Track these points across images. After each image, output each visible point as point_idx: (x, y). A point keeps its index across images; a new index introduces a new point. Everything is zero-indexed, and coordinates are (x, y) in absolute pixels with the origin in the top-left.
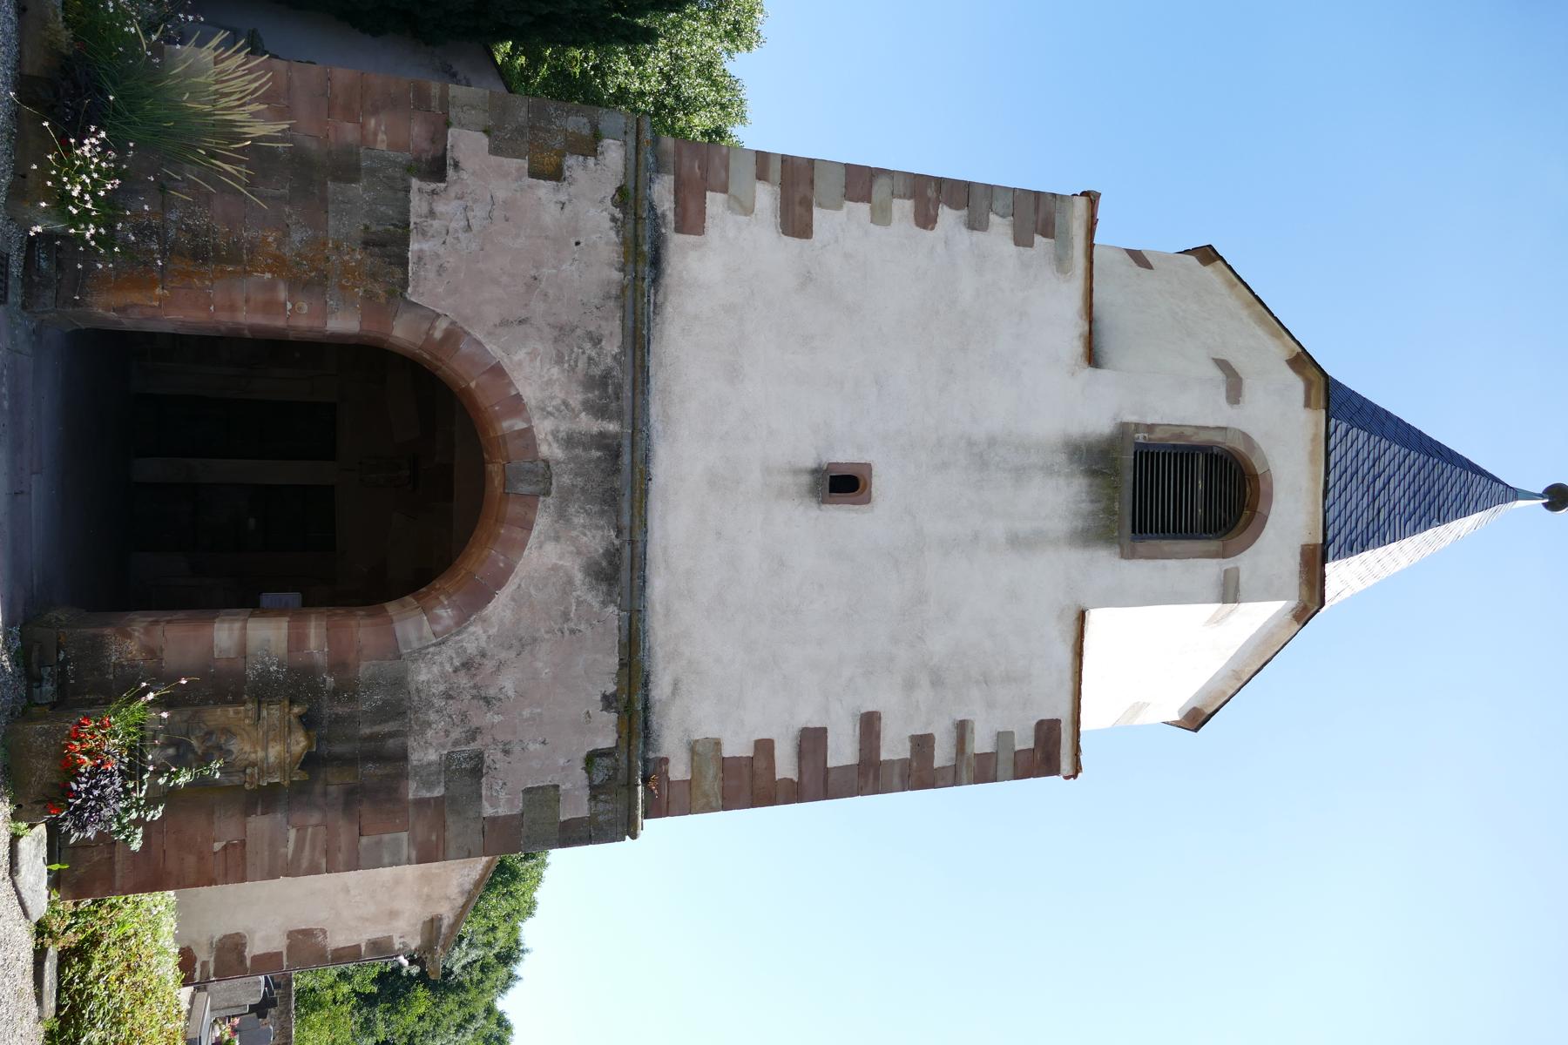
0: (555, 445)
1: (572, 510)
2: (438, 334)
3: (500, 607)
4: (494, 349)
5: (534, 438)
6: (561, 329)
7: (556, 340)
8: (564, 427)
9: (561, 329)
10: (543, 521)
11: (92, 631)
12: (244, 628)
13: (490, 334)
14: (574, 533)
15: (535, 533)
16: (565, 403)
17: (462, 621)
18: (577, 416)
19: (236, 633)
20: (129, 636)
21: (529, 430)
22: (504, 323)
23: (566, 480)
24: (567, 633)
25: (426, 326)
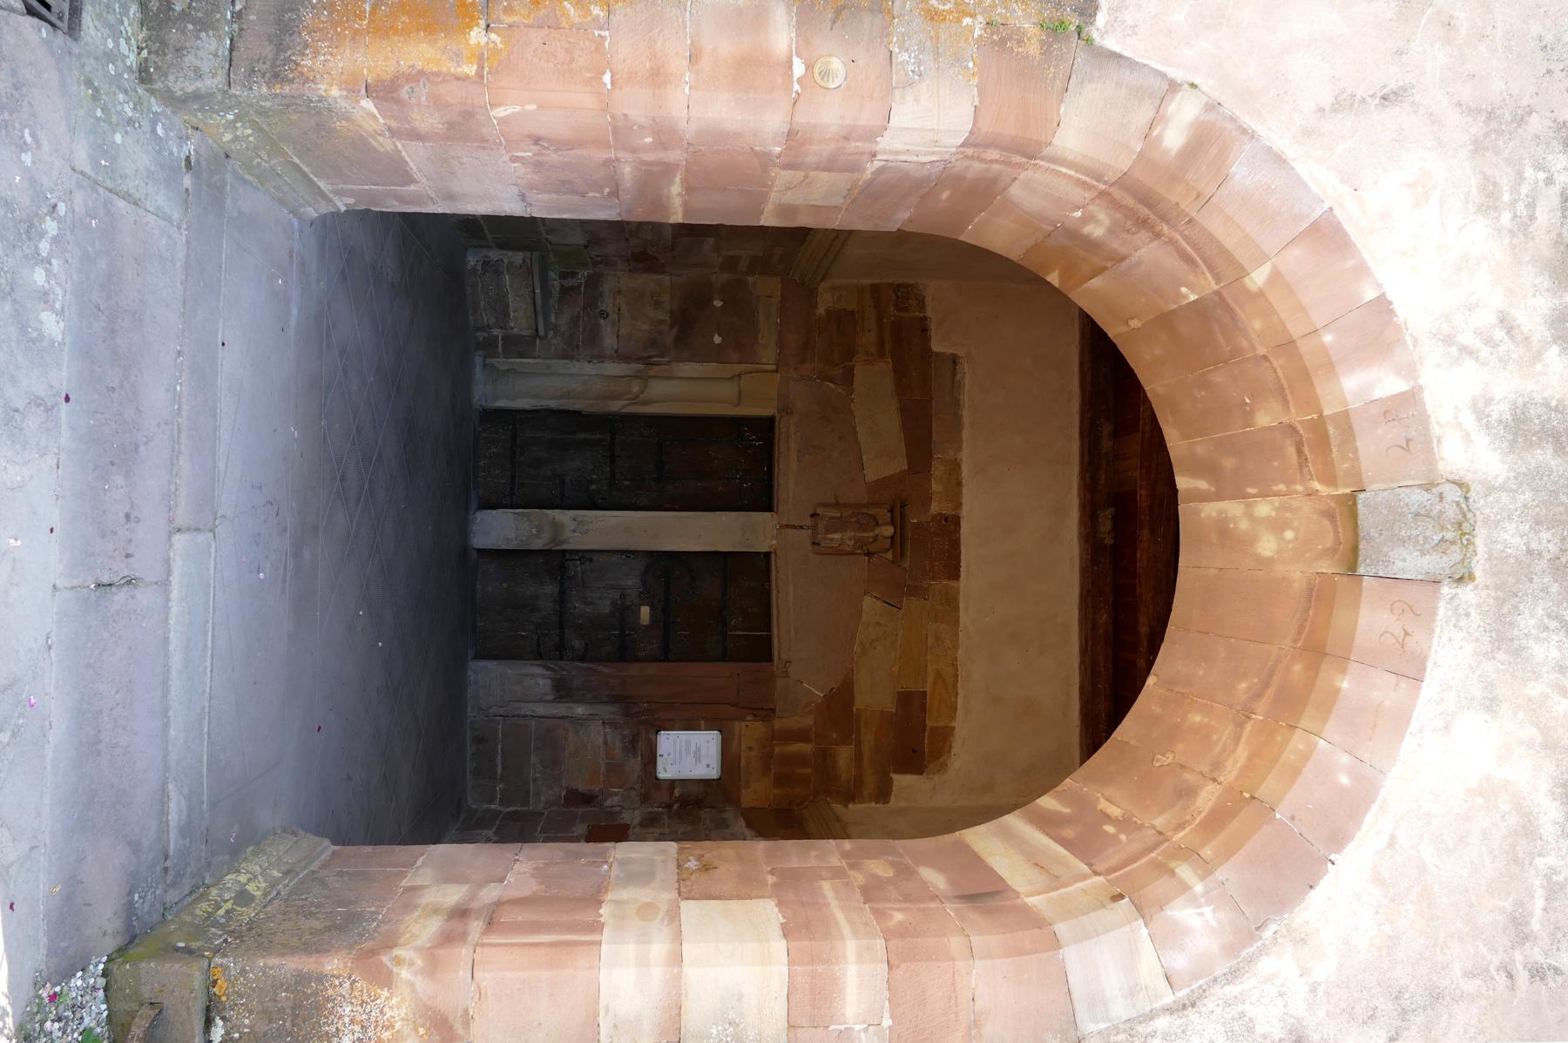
0: (1481, 440)
1: (1528, 621)
2: (1173, 138)
3: (1343, 908)
4: (1321, 180)
5: (1424, 420)
6: (1491, 116)
7: (1478, 148)
8: (1506, 387)
9: (1491, 116)
10: (1453, 647)
11: (292, 964)
12: (677, 959)
13: (1308, 133)
14: (1535, 689)
15: (1428, 689)
16: (1506, 322)
17: (1243, 939)
18: (1537, 357)
19: (657, 973)
20: (385, 979)
21: (1411, 398)
22: (1345, 103)
23: (1512, 537)
24: (1522, 976)
25: (1143, 115)
